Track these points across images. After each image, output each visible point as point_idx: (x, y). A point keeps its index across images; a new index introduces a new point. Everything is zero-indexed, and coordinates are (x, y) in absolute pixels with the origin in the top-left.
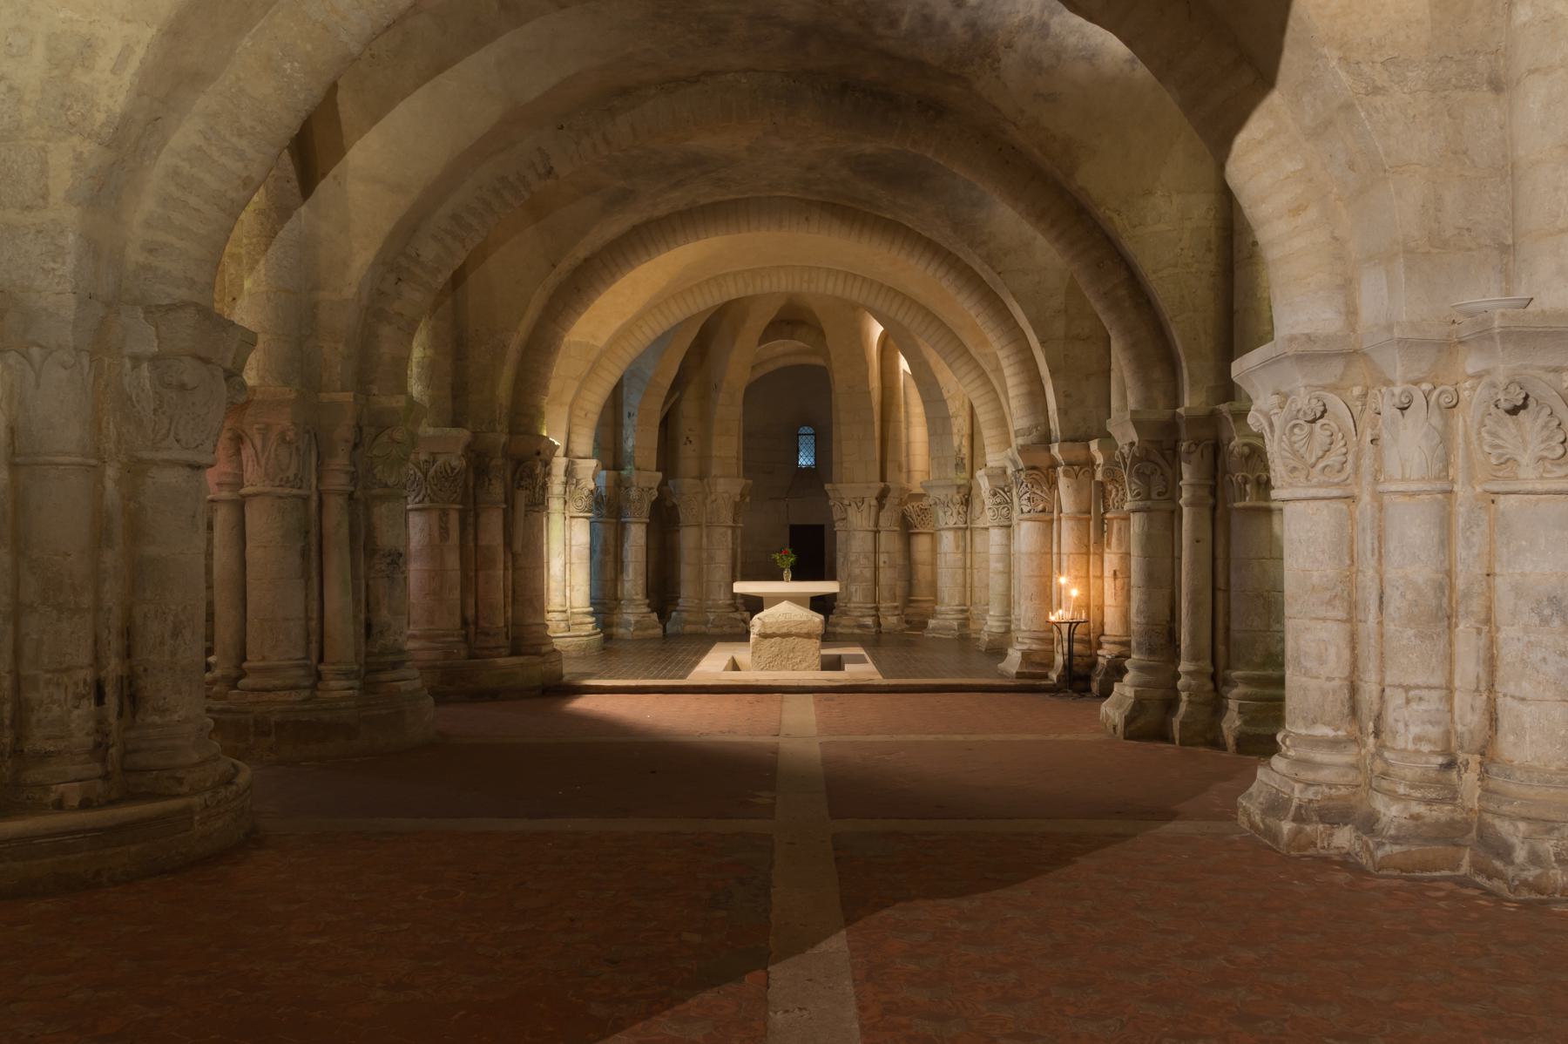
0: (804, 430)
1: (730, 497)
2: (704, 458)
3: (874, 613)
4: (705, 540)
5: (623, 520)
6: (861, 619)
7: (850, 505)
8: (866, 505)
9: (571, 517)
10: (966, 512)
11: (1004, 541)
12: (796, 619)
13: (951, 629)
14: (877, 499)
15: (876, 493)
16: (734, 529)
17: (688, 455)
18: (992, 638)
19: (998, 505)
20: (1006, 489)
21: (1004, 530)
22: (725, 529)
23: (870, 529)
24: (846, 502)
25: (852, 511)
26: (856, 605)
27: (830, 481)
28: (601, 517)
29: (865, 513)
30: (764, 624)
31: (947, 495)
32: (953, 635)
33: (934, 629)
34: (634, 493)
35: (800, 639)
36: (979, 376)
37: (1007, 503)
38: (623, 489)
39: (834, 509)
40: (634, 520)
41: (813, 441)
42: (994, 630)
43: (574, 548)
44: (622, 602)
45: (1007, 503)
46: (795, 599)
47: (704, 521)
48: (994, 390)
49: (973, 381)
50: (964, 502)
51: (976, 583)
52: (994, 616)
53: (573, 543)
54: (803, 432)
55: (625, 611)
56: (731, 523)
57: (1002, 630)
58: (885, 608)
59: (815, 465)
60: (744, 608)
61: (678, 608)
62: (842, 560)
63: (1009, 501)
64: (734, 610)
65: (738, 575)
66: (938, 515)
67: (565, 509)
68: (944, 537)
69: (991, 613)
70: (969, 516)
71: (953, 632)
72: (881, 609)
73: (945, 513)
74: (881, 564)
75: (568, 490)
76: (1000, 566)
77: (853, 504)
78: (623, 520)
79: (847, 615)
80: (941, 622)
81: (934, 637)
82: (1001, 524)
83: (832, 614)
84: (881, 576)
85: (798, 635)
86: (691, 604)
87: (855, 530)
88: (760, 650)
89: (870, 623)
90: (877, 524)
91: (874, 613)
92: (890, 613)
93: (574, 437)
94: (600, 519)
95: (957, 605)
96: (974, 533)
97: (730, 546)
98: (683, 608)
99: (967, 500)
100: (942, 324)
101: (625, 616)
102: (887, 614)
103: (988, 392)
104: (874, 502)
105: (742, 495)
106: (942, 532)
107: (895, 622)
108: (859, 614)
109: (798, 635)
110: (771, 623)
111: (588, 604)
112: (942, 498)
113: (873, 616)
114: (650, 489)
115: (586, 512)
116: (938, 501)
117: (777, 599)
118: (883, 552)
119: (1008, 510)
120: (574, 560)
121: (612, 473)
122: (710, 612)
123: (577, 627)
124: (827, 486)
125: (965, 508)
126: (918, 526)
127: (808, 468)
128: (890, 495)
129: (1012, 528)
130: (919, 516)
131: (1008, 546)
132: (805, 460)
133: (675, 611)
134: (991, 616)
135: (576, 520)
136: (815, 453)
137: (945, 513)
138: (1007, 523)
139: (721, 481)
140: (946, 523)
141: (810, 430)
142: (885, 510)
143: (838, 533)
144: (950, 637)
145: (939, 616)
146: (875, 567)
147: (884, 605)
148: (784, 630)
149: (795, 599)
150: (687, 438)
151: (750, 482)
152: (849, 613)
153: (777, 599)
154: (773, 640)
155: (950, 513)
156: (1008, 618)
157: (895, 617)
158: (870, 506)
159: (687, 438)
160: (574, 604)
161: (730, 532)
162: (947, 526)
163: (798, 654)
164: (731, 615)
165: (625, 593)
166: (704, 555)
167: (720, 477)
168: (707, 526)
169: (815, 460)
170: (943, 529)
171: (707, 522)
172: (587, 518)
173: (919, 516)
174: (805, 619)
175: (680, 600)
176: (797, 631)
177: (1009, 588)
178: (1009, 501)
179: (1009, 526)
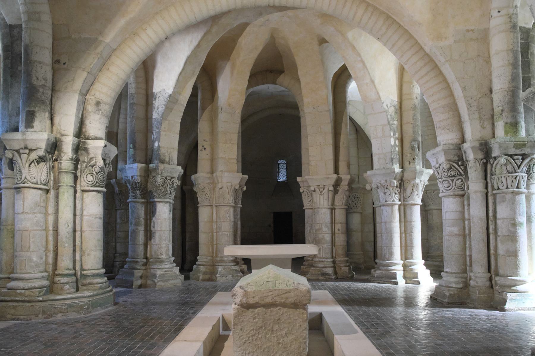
0: (280, 162)
2: (213, 160)
3: (333, 265)
4: (214, 215)
5: (152, 200)
6: (324, 269)
7: (315, 191)
8: (326, 190)
9: (83, 191)
10: (400, 193)
11: (459, 208)
12: (281, 287)
14: (333, 186)
15: (332, 182)
16: (234, 207)
17: (203, 156)
18: (452, 293)
19: (452, 177)
21: (458, 199)
22: (228, 208)
23: (329, 207)
24: (312, 189)
25: (316, 196)
26: (320, 260)
27: (300, 175)
28: (136, 198)
29: (326, 196)
30: (246, 294)
31: (386, 181)
34: (159, 180)
35: (285, 310)
36: (432, 69)
37: (461, 175)
38: (152, 177)
39: (303, 195)
40: (159, 200)
41: (285, 167)
42: (454, 285)
43: (85, 218)
44: (151, 260)
46: (279, 262)
47: (214, 203)
48: (445, 80)
49: (426, 74)
50: (398, 185)
52: (452, 273)
53: (85, 213)
54: (280, 163)
55: (152, 267)
56: (233, 204)
57: (461, 286)
58: (340, 261)
59: (287, 180)
60: (243, 262)
61: (197, 263)
62: (309, 228)
63: (463, 173)
64: (235, 264)
65: (239, 240)
66: (379, 195)
67: (75, 183)
68: (384, 211)
69: (446, 270)
70: (402, 195)
72: (337, 262)
73: (385, 193)
74: (337, 231)
75: (79, 167)
76: (455, 230)
77: (317, 190)
78: (152, 200)
79: (314, 267)
80: (384, 272)
82: (456, 193)
83: (303, 265)
84: (336, 239)
85: (284, 305)
86: (206, 260)
87: (318, 208)
88: (243, 321)
89: (330, 272)
90: (333, 204)
91: (333, 265)
92: (343, 265)
93: (87, 122)
94: (135, 200)
96: (406, 207)
97: (232, 220)
98: (201, 263)
99: (400, 184)
100: (400, 26)
101: (152, 271)
102: (341, 265)
103: (440, 82)
104: (331, 188)
105: (240, 185)
106: (382, 208)
107: (347, 271)
108: (322, 266)
109: (284, 305)
110: (254, 292)
111: (100, 265)
112: (382, 182)
113: (332, 267)
114: (172, 178)
115: (97, 186)
116: (379, 185)
117: (264, 262)
118: (337, 223)
119: (462, 181)
120: (85, 228)
121: (143, 165)
122: (219, 266)
123: (85, 288)
124: (299, 179)
125: (399, 189)
126: (353, 208)
127: (283, 182)
128: (342, 184)
129: (466, 197)
130: (353, 202)
131: (463, 212)
132: (282, 177)
133: (195, 264)
134: (447, 272)
135: (87, 193)
136: (287, 174)
137: (385, 193)
138: (461, 193)
139: (226, 174)
140: (386, 201)
141: (283, 161)
142: (338, 194)
143: (306, 210)
145: (381, 268)
146: (332, 233)
147: (339, 259)
148: (268, 300)
149: (279, 262)
150: (203, 146)
151: (247, 176)
152: (315, 265)
153: (264, 262)
154: (256, 311)
156: (465, 275)
157: (347, 268)
158: (329, 191)
159: (203, 146)
160: (85, 267)
161: (232, 210)
163: (285, 325)
165: (153, 254)
166: (215, 226)
167: (224, 172)
168: (216, 206)
169: (287, 178)
170: (384, 205)
171: (216, 203)
172: (99, 192)
173: (353, 202)
175: (198, 257)
176: (283, 301)
177: (464, 249)
178: (463, 173)
179: (463, 196)
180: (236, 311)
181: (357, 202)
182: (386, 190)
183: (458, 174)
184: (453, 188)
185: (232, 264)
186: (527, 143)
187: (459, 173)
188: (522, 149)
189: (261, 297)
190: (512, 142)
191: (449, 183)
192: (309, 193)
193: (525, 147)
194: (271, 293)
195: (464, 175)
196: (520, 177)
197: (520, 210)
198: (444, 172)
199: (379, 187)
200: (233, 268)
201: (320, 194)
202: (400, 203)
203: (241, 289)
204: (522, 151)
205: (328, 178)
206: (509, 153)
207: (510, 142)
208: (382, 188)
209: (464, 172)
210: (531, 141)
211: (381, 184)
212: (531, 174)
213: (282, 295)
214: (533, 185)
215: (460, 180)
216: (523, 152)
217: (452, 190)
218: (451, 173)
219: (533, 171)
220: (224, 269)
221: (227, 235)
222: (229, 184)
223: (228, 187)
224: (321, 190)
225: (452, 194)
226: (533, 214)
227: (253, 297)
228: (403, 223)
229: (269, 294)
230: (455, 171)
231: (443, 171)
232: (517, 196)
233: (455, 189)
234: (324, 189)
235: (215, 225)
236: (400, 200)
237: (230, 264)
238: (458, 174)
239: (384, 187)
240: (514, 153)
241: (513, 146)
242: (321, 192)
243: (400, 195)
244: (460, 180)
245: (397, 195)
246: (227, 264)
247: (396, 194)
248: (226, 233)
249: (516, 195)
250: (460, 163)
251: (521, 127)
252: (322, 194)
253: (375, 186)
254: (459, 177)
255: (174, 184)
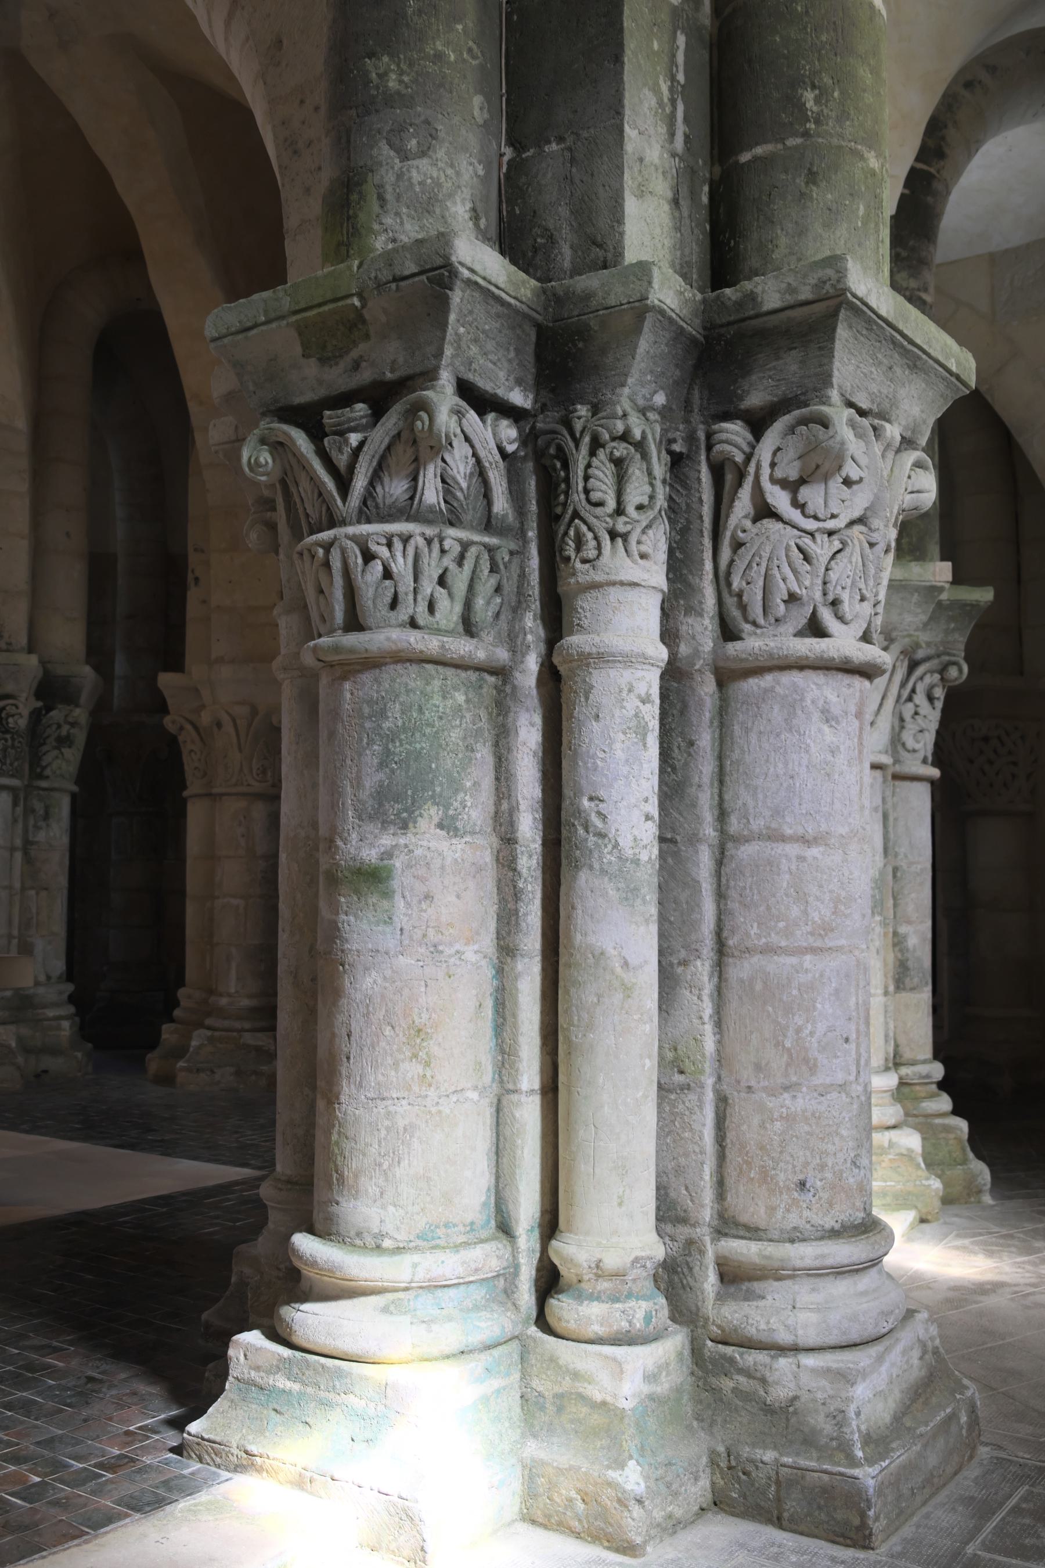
130: (971, 762)
181: (991, 762)
185: (247, 1025)
186: (356, 302)
188: (354, 354)
190: (282, 317)
193: (367, 337)
196: (343, 551)
197: (359, 777)
200: (249, 1039)
204: (356, 366)
206: (298, 400)
207: (267, 322)
210: (380, 286)
212: (576, 515)
214: (594, 593)
216: (366, 376)
219: (587, 491)
220: (211, 1040)
223: (238, 722)
226: (586, 803)
232: (347, 685)
237: (237, 1025)
240: (322, 392)
241: (299, 350)
246: (227, 1023)
249: (344, 678)
251: (376, 208)
255: (11, 720)
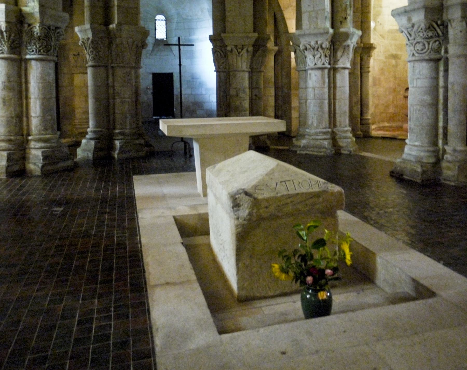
1: (134, 42)
12: (303, 190)
13: (320, 147)
19: (429, 38)
20: (439, 22)
21: (432, 64)
22: (128, 70)
32: (325, 152)
33: (305, 147)
45: (439, 36)
51: (337, 111)
71: (324, 150)
81: (307, 154)
87: (237, 71)
95: (324, 128)
104: (251, 49)
112: (313, 43)
116: (308, 46)
119: (440, 43)
140: (315, 64)
144: (322, 154)
155: (318, 56)
162: (316, 66)
164: (137, 142)
174: (316, 189)
179: (437, 60)
180: (240, 229)
182: (316, 53)
183: (435, 35)
184: (429, 51)
187: (437, 34)
189: (277, 207)
191: (424, 45)
192: (222, 53)
194: (292, 199)
195: (442, 36)
198: (420, 32)
199: (308, 49)
201: (238, 55)
202: (329, 66)
203: (247, 197)
205: (247, 37)
208: (312, 50)
209: (443, 33)
211: (310, 45)
213: (307, 202)
215: (437, 43)
217: (427, 53)
218: (428, 34)
221: (129, 102)
222: (130, 40)
224: (239, 50)
225: (427, 58)
227: (267, 207)
228: (332, 89)
229: (289, 200)
230: (432, 32)
231: (418, 31)
233: (430, 52)
234: (242, 50)
235: (112, 90)
236: (330, 64)
238: (435, 35)
239: (314, 49)
242: (239, 53)
243: (330, 58)
244: (437, 43)
245: (327, 58)
247: (326, 56)
248: (128, 100)
250: (439, 22)
252: (240, 55)
253: (304, 47)
254: (437, 39)
